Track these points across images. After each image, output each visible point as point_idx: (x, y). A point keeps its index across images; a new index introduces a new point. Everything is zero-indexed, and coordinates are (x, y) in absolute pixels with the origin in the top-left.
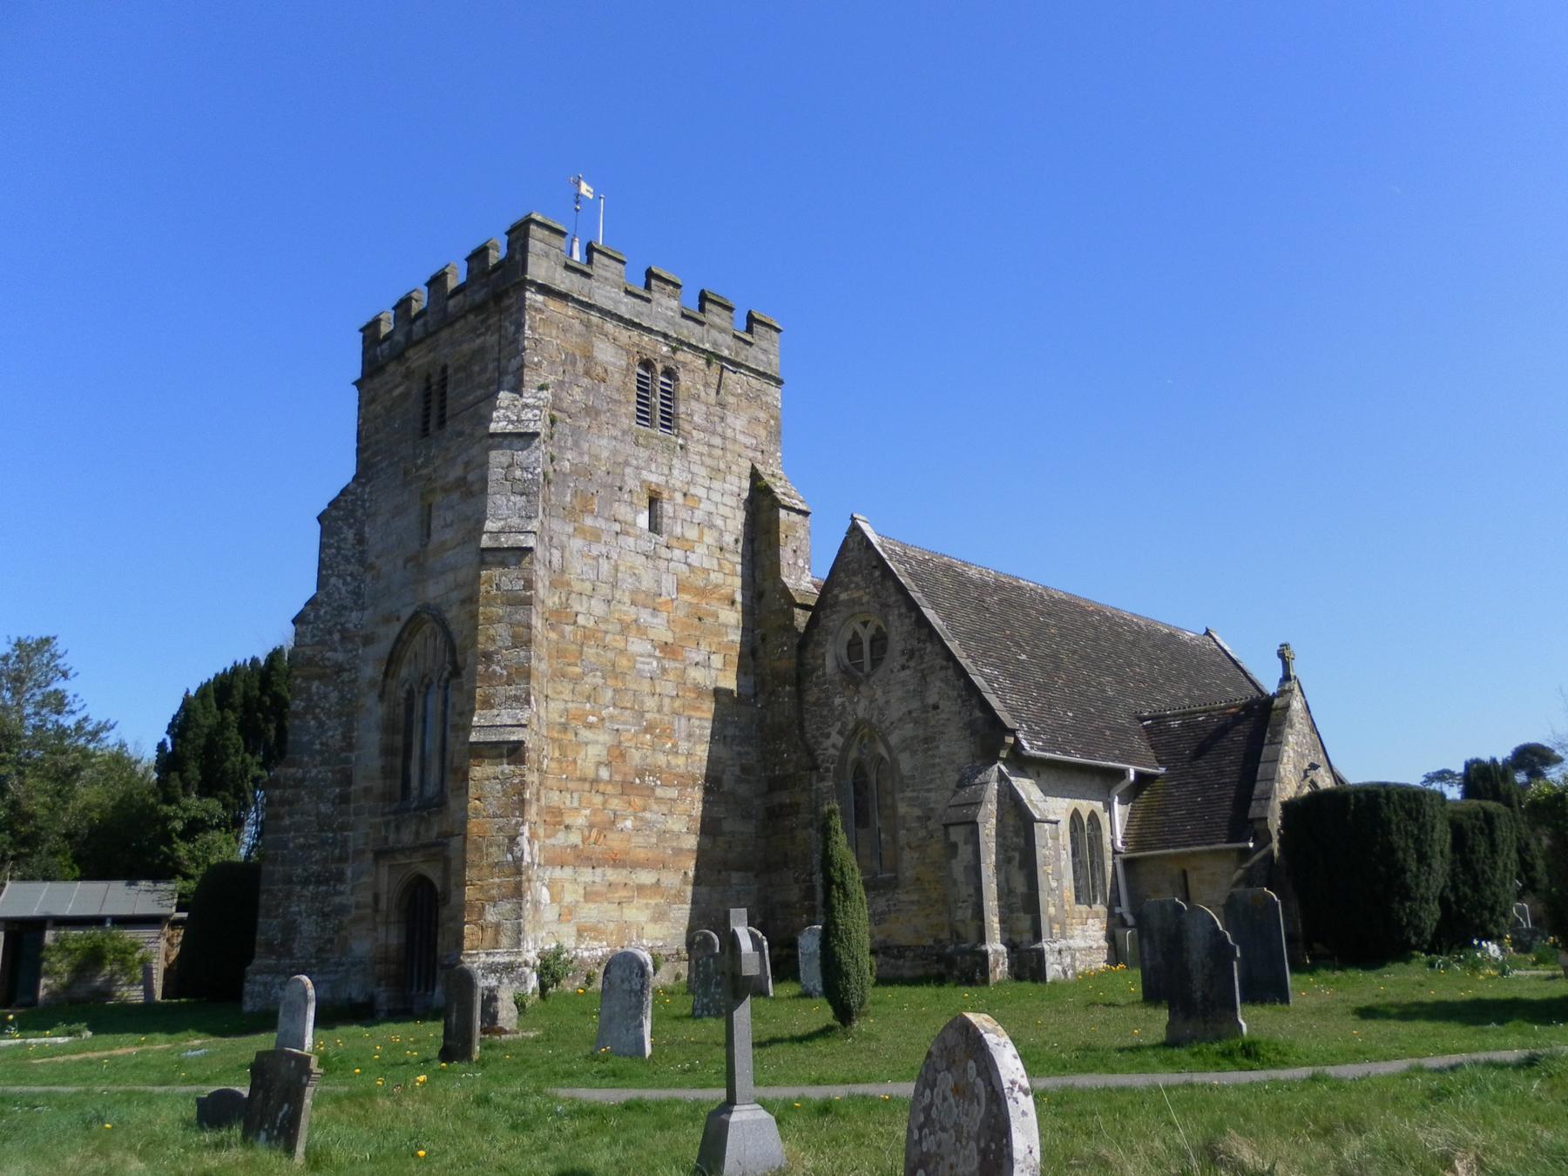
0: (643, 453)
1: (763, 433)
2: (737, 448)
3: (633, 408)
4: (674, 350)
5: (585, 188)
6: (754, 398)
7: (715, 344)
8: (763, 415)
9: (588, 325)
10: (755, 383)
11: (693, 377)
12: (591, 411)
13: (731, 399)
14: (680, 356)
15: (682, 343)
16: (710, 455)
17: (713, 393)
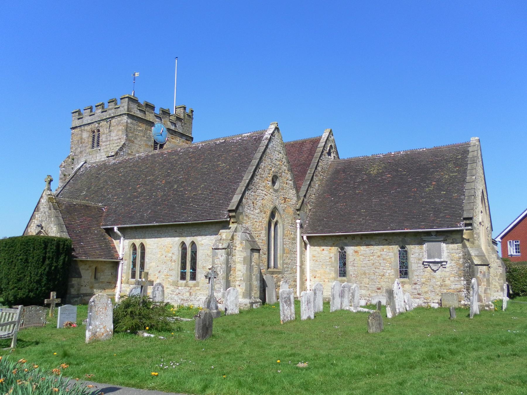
0: (91, 156)
1: (120, 133)
2: (113, 142)
3: (90, 146)
4: (99, 124)
5: (137, 74)
6: (118, 124)
7: (110, 114)
8: (120, 128)
9: (81, 131)
10: (119, 119)
11: (104, 127)
12: (81, 152)
13: (112, 128)
14: (101, 124)
15: (100, 121)
16: (106, 148)
17: (108, 129)
